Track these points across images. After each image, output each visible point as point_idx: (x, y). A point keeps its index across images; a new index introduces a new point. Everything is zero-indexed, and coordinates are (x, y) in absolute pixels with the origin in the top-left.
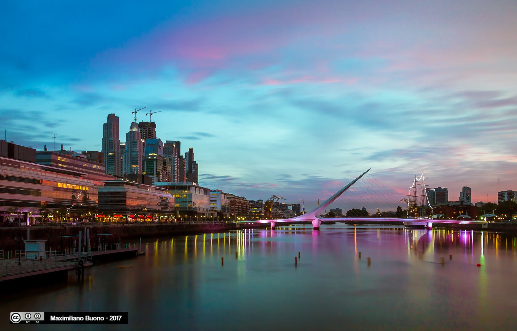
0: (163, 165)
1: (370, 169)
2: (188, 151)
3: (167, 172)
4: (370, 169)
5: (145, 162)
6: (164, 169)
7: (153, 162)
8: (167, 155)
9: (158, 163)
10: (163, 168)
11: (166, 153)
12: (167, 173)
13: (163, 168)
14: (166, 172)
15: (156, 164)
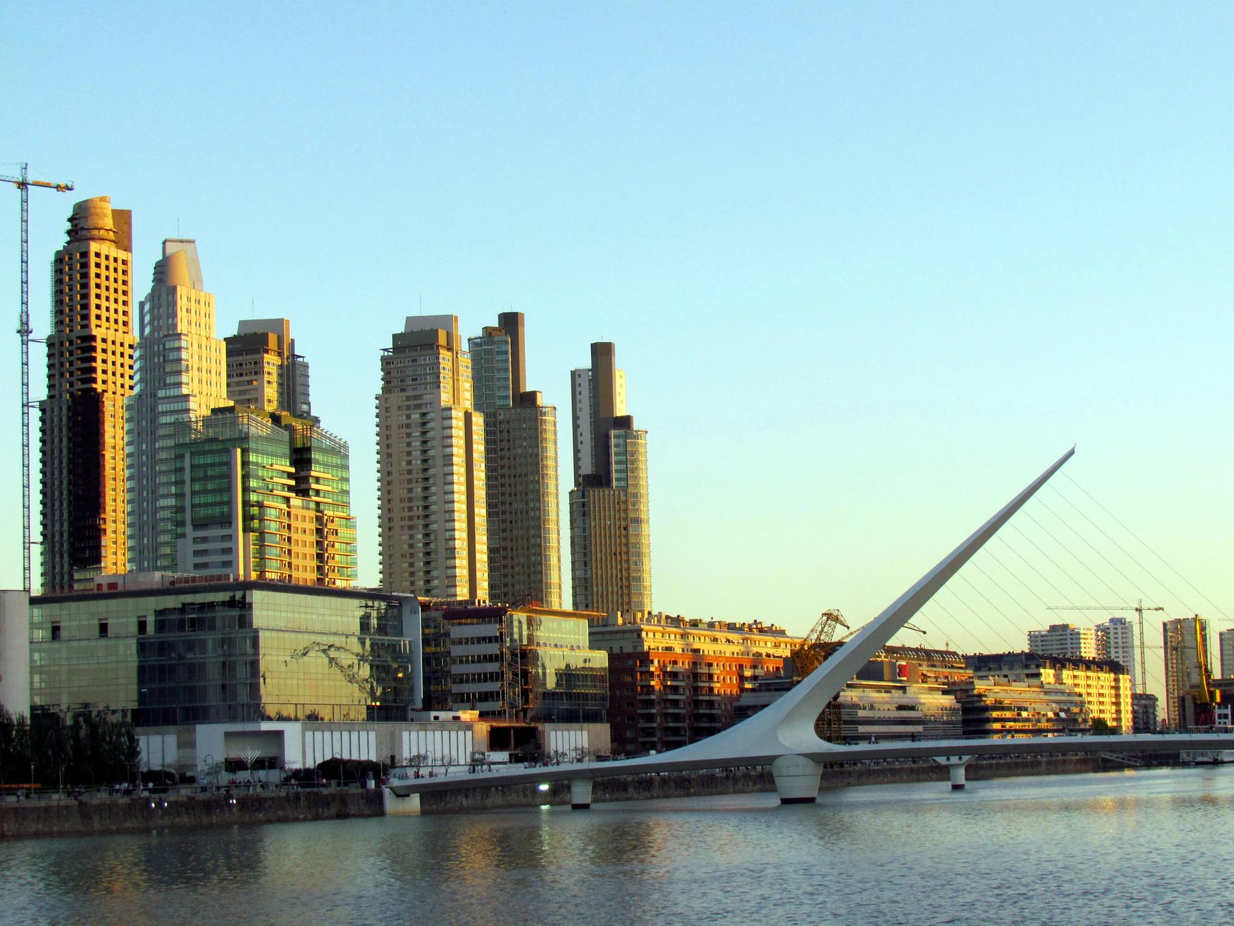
0: (291, 465)
1: (1072, 453)
2: (585, 361)
3: (318, 504)
4: (1072, 453)
5: (188, 456)
6: (303, 486)
7: (228, 452)
8: (408, 398)
9: (253, 458)
10: (293, 483)
11: (403, 390)
12: (322, 507)
13: (293, 483)
14: (313, 505)
15: (245, 464)
